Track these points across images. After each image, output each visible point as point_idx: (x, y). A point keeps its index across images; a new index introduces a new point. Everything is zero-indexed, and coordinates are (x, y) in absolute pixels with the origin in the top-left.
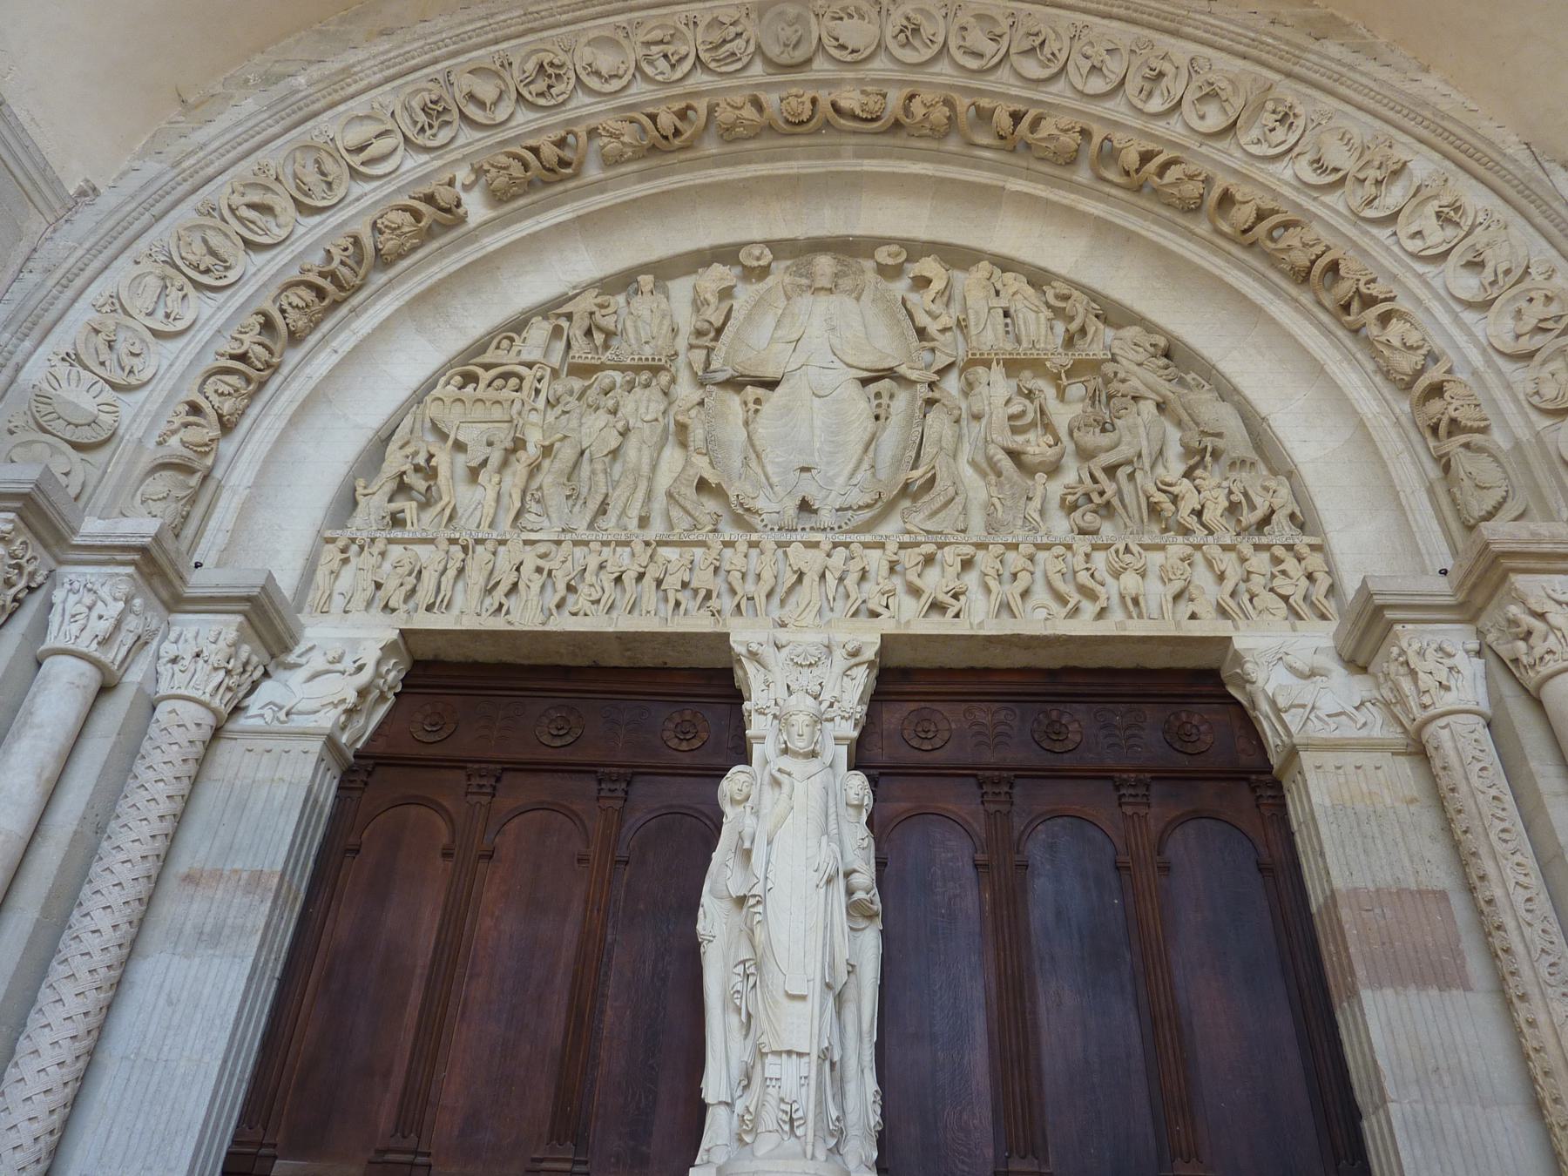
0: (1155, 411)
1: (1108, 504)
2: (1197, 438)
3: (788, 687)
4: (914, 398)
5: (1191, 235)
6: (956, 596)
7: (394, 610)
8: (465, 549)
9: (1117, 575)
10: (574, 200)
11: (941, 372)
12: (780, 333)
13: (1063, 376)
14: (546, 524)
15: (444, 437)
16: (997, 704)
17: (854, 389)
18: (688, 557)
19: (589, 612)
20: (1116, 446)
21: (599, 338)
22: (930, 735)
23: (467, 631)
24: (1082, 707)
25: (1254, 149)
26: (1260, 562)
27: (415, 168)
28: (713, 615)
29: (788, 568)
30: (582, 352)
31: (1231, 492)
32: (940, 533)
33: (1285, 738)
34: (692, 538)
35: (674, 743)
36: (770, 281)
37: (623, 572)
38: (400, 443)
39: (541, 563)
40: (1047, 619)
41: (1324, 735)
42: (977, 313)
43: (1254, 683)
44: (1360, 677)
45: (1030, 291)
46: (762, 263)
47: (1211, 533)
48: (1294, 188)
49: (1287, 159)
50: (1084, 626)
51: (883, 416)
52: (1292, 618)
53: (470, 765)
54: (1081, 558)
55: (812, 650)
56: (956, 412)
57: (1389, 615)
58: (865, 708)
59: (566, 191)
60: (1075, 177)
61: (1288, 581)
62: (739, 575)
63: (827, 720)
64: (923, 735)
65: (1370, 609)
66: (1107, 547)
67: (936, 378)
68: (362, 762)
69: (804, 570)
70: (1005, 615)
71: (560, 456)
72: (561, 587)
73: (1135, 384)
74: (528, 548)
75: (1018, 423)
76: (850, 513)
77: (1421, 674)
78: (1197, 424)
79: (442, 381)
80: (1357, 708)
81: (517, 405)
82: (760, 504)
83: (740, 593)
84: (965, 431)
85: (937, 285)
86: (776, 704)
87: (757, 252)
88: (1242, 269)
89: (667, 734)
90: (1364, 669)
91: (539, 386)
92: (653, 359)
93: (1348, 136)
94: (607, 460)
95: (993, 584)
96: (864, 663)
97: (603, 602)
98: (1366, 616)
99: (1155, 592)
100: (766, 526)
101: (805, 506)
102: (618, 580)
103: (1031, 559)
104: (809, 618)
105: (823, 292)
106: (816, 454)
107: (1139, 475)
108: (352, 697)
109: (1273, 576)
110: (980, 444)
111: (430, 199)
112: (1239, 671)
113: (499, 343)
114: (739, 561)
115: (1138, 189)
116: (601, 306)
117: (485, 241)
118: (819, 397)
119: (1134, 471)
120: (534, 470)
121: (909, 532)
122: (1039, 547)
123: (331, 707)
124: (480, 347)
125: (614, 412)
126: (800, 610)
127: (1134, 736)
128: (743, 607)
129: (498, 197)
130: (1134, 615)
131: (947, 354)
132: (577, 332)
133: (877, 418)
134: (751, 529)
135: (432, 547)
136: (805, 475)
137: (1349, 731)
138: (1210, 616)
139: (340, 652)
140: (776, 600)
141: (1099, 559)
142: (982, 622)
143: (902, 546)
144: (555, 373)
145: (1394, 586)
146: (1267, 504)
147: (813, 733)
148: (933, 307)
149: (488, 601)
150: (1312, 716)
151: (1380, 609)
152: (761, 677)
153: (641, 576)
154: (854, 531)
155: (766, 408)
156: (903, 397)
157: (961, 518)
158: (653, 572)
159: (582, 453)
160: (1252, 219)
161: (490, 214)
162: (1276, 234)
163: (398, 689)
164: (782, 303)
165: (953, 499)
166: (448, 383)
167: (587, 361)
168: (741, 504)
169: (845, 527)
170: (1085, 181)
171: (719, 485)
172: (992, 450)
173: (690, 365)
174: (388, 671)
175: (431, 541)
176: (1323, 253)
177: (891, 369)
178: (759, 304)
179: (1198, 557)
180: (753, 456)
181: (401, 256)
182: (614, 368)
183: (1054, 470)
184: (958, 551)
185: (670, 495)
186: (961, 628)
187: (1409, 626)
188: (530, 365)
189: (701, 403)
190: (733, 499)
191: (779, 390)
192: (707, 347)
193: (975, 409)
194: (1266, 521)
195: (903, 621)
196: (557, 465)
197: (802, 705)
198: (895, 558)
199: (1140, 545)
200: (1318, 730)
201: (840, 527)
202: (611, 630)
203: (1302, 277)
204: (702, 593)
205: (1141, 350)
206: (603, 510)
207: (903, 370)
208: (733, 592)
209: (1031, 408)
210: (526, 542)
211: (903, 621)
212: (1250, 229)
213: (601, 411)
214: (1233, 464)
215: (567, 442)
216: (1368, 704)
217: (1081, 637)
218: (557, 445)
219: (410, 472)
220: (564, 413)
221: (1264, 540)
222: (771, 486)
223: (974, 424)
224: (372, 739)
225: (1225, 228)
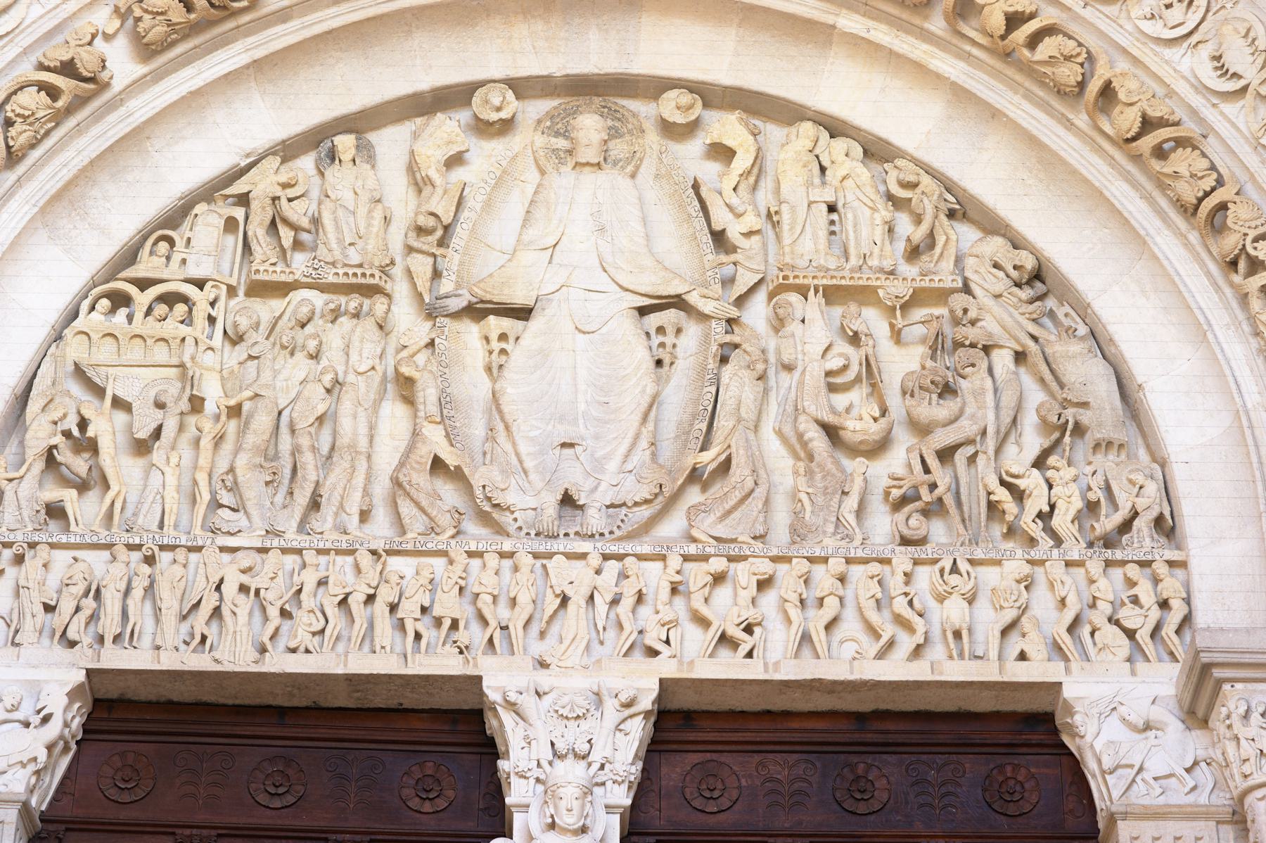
0: (1012, 366)
1: (940, 500)
2: (1057, 409)
3: (553, 744)
4: (706, 338)
5: (1069, 125)
6: (749, 630)
7: (72, 644)
8: (150, 560)
9: (941, 599)
10: (246, 36)
11: (740, 301)
12: (531, 233)
13: (898, 312)
14: (244, 522)
15: (99, 392)
16: (795, 756)
17: (627, 327)
18: (426, 574)
19: (311, 648)
20: (956, 419)
21: (287, 235)
22: (716, 794)
23: (168, 672)
24: (892, 759)
25: (1149, 27)
26: (1109, 586)
27: (41, 17)
28: (461, 652)
29: (549, 591)
30: (266, 266)
31: (1090, 489)
32: (734, 541)
33: (1108, 803)
34: (430, 545)
35: (414, 803)
36: (516, 142)
37: (348, 595)
38: (42, 402)
39: (245, 579)
40: (854, 659)
41: (1146, 801)
42: (793, 209)
43: (1082, 737)
44: (1198, 732)
45: (863, 173)
46: (504, 115)
47: (1058, 541)
48: (1193, 85)
49: (1185, 45)
50: (896, 669)
51: (667, 361)
52: (1139, 657)
53: (178, 831)
54: (900, 578)
55: (581, 701)
56: (760, 367)
57: (1217, 673)
58: (640, 765)
59: (238, 27)
60: (927, 25)
61: (1137, 610)
62: (489, 599)
63: (597, 784)
64: (708, 794)
65: (1198, 666)
66: (935, 561)
67: (734, 313)
68: (51, 827)
69: (569, 593)
70: (806, 652)
71: (254, 425)
72: (273, 612)
73: (990, 326)
74: (226, 557)
75: (838, 380)
76: (624, 510)
77: (1243, 742)
78: (1062, 386)
80: (1188, 770)
81: (189, 341)
82: (510, 498)
83: (493, 624)
84: (772, 382)
85: (742, 161)
86: (539, 765)
87: (496, 101)
88: (1127, 180)
89: (406, 792)
90: (1204, 723)
91: (214, 314)
92: (364, 275)
93: (1252, 34)
94: (312, 430)
95: (794, 613)
96: (639, 714)
97: (328, 632)
98: (1196, 672)
99: (988, 620)
100: (520, 528)
101: (567, 500)
102: (344, 602)
103: (842, 579)
104: (575, 656)
105: (588, 169)
106: (581, 421)
107: (981, 460)
108: (42, 755)
109: (1123, 604)
110: (790, 409)
111: (68, 69)
112: (1069, 720)
113: (155, 244)
114: (489, 579)
115: (1007, 55)
116: (285, 186)
117: (132, 104)
118: (584, 333)
119: (976, 453)
120: (219, 440)
121: (694, 540)
122: (849, 561)
123: (19, 766)
124: (130, 256)
125: (315, 357)
126: (563, 647)
127: (948, 794)
128: (496, 641)
129: (147, 50)
130: (955, 654)
131: (751, 270)
132: (258, 229)
133: (659, 363)
134: (500, 530)
135: (106, 554)
136: (568, 452)
137: (1178, 796)
138: (1040, 657)
139: (18, 699)
140: (535, 629)
141: (924, 576)
142: (777, 664)
143: (686, 558)
144: (232, 291)
145: (1223, 642)
146: (1129, 505)
147: (583, 806)
148: (734, 200)
149: (185, 628)
150: (1138, 779)
151: (1207, 668)
152: (520, 732)
153: (370, 599)
154: (630, 536)
155: (518, 355)
156: (693, 331)
157: (761, 519)
158: (386, 595)
159: (280, 413)
160: (1135, 129)
161: (141, 70)
162: (1166, 146)
163: (79, 738)
164: (533, 176)
165: (752, 491)
166: (92, 308)
167: (275, 278)
168: (489, 499)
169: (618, 533)
170: (940, 33)
171: (458, 468)
172: (802, 427)
173: (409, 272)
174: (74, 717)
175: (109, 546)
176: (1213, 189)
177: (679, 296)
178: (502, 179)
179: (1039, 571)
180: (500, 427)
181: (32, 146)
183: (879, 448)
184: (754, 569)
185: (397, 483)
186: (753, 671)
187: (1239, 686)
188: (200, 284)
189: (431, 344)
190: (478, 492)
191: (536, 323)
192: (435, 256)
193: (786, 358)
194: (1126, 526)
195: (686, 660)
196: (251, 440)
197: (571, 774)
198: (678, 578)
199: (972, 562)
200: (1144, 795)
201: (611, 532)
202: (340, 670)
203: (1190, 211)
204: (447, 623)
205: (1001, 274)
206: (315, 504)
207: (693, 299)
208: (484, 622)
209: (855, 355)
210: (223, 549)
211: (686, 660)
212: (1134, 139)
213: (300, 356)
214: (1097, 446)
215: (261, 403)
216: (1203, 764)
217: (890, 682)
218: (246, 407)
220: (251, 357)
221: (1118, 555)
222: (525, 472)
223: (784, 375)
224: (55, 799)
225: (1107, 128)
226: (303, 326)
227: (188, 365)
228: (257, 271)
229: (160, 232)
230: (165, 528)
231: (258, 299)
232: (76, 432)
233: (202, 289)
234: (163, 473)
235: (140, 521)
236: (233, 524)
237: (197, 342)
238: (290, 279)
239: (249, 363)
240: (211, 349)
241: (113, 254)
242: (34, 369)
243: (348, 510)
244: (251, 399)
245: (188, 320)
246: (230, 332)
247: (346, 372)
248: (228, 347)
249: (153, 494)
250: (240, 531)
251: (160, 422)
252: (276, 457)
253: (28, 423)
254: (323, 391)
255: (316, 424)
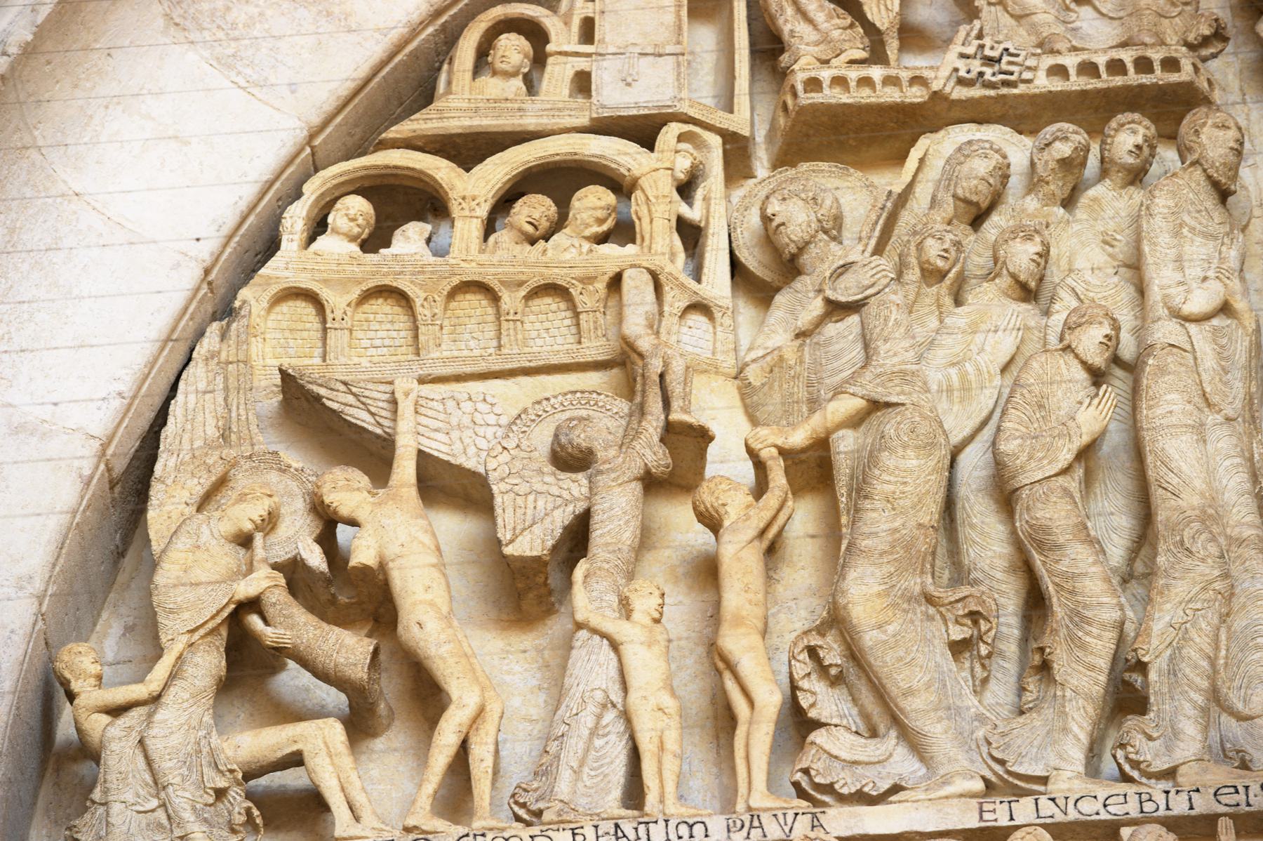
14: (903, 764)
38: (197, 486)
79: (296, 218)
81: (637, 289)
91: (694, 213)
92: (1144, 65)
94: (1073, 483)
166: (319, 226)
167: (864, 96)
182: (978, 114)
215: (890, 424)
218: (846, 444)
219: (278, 598)
226: (978, 218)
227: (645, 344)
228: (814, 84)
229: (498, 12)
230: (651, 799)
231: (824, 165)
232: (315, 558)
233: (648, 143)
234: (615, 646)
235: (563, 787)
236: (870, 772)
237: (658, 288)
238: (916, 95)
239: (831, 329)
240: (700, 307)
241: (363, 71)
242: (157, 402)
243: (1240, 706)
244: (856, 421)
245: (623, 232)
246: (752, 260)
247: (1140, 331)
248: (746, 312)
249: (592, 708)
250: (896, 789)
251: (580, 507)
252: (960, 574)
253: (156, 547)
254: (1081, 375)
255: (1079, 472)
